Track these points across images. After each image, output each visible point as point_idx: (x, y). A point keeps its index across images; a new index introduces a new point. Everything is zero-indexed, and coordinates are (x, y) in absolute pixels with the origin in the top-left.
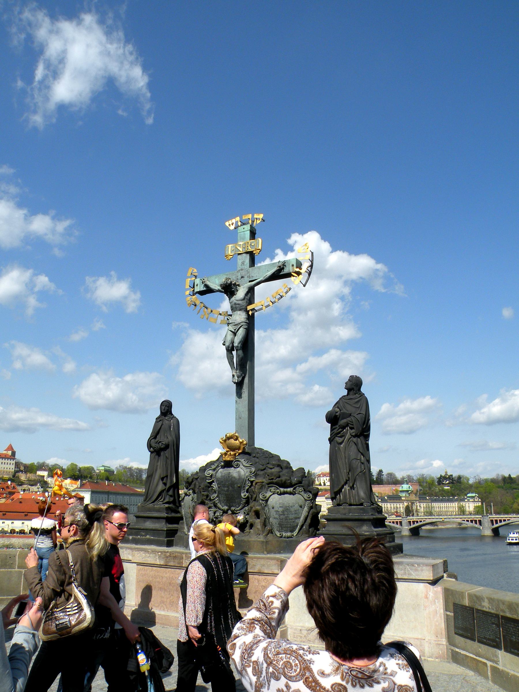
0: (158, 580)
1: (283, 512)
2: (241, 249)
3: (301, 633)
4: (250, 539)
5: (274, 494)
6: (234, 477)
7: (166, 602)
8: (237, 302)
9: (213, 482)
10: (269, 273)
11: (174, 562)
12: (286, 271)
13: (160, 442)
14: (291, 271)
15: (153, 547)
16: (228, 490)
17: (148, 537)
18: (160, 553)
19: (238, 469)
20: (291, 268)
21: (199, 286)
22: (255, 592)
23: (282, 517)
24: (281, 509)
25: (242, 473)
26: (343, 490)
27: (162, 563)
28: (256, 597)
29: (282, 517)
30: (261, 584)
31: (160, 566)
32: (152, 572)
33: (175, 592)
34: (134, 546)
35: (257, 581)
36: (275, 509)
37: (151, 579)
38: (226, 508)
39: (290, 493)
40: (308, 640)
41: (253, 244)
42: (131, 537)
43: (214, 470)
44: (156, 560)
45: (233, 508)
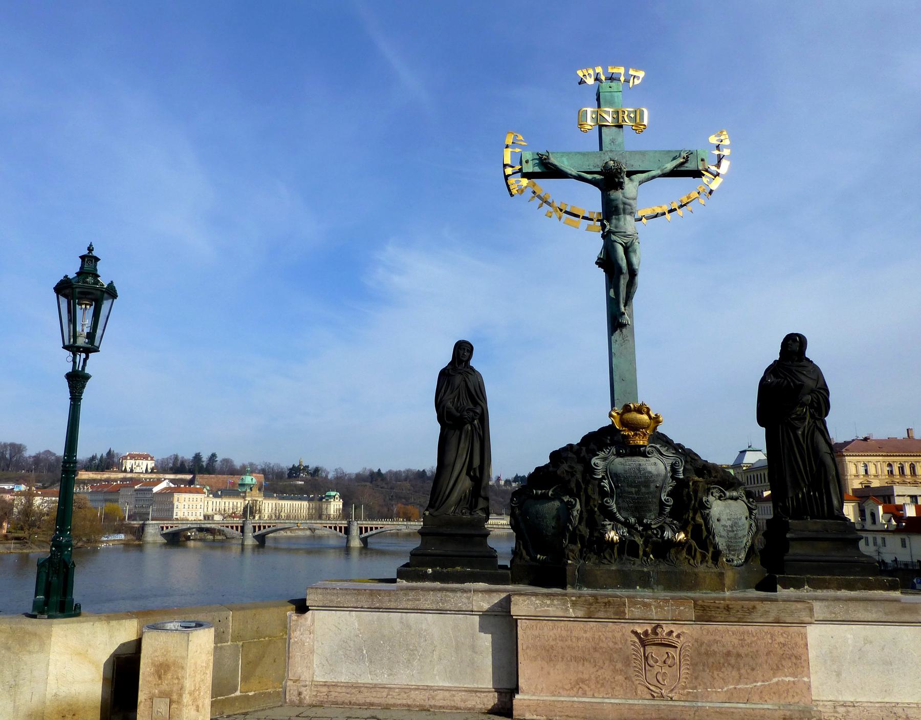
0: (569, 643)
1: (732, 527)
4: (696, 570)
6: (650, 472)
7: (589, 679)
10: (670, 166)
11: (606, 611)
16: (636, 493)
18: (574, 598)
22: (768, 654)
23: (731, 534)
24: (729, 523)
27: (580, 613)
28: (770, 661)
29: (731, 534)
30: (778, 641)
31: (576, 619)
32: (555, 631)
33: (607, 663)
34: (438, 584)
35: (769, 636)
36: (723, 522)
37: (553, 643)
39: (736, 499)
44: (567, 610)
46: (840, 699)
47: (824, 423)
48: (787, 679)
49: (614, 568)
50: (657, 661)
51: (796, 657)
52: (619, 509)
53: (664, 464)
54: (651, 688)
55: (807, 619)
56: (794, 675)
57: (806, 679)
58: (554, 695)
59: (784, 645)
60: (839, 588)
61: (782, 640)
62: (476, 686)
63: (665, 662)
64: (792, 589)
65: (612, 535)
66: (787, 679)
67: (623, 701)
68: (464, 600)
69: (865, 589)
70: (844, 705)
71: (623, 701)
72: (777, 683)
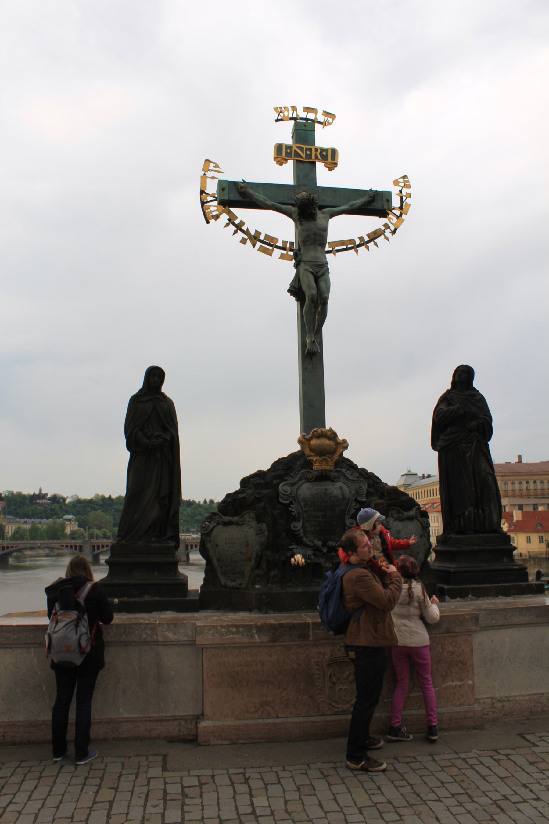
2: (303, 155)
3: (493, 707)
5: (395, 520)
6: (336, 497)
8: (319, 232)
9: (291, 503)
12: (377, 205)
13: (158, 436)
14: (386, 207)
15: (169, 615)
17: (147, 598)
19: (339, 484)
20: (385, 203)
21: (227, 190)
25: (346, 490)
26: (466, 514)
35: (440, 646)
38: (319, 543)
40: (504, 715)
41: (324, 153)
42: (116, 600)
43: (294, 484)
44: (252, 636)
45: (331, 543)
46: (497, 695)
47: (487, 446)
48: (454, 684)
49: (299, 590)
50: (339, 679)
51: (463, 663)
52: (305, 532)
53: (349, 488)
54: (334, 704)
55: (474, 628)
56: (460, 680)
57: (470, 682)
58: (239, 719)
59: (453, 653)
60: (496, 595)
61: (451, 648)
62: (161, 714)
63: (347, 678)
64: (458, 599)
65: (299, 558)
66: (454, 684)
67: (306, 719)
68: (149, 632)
69: (517, 594)
70: (500, 701)
71: (306, 719)
72: (446, 689)
